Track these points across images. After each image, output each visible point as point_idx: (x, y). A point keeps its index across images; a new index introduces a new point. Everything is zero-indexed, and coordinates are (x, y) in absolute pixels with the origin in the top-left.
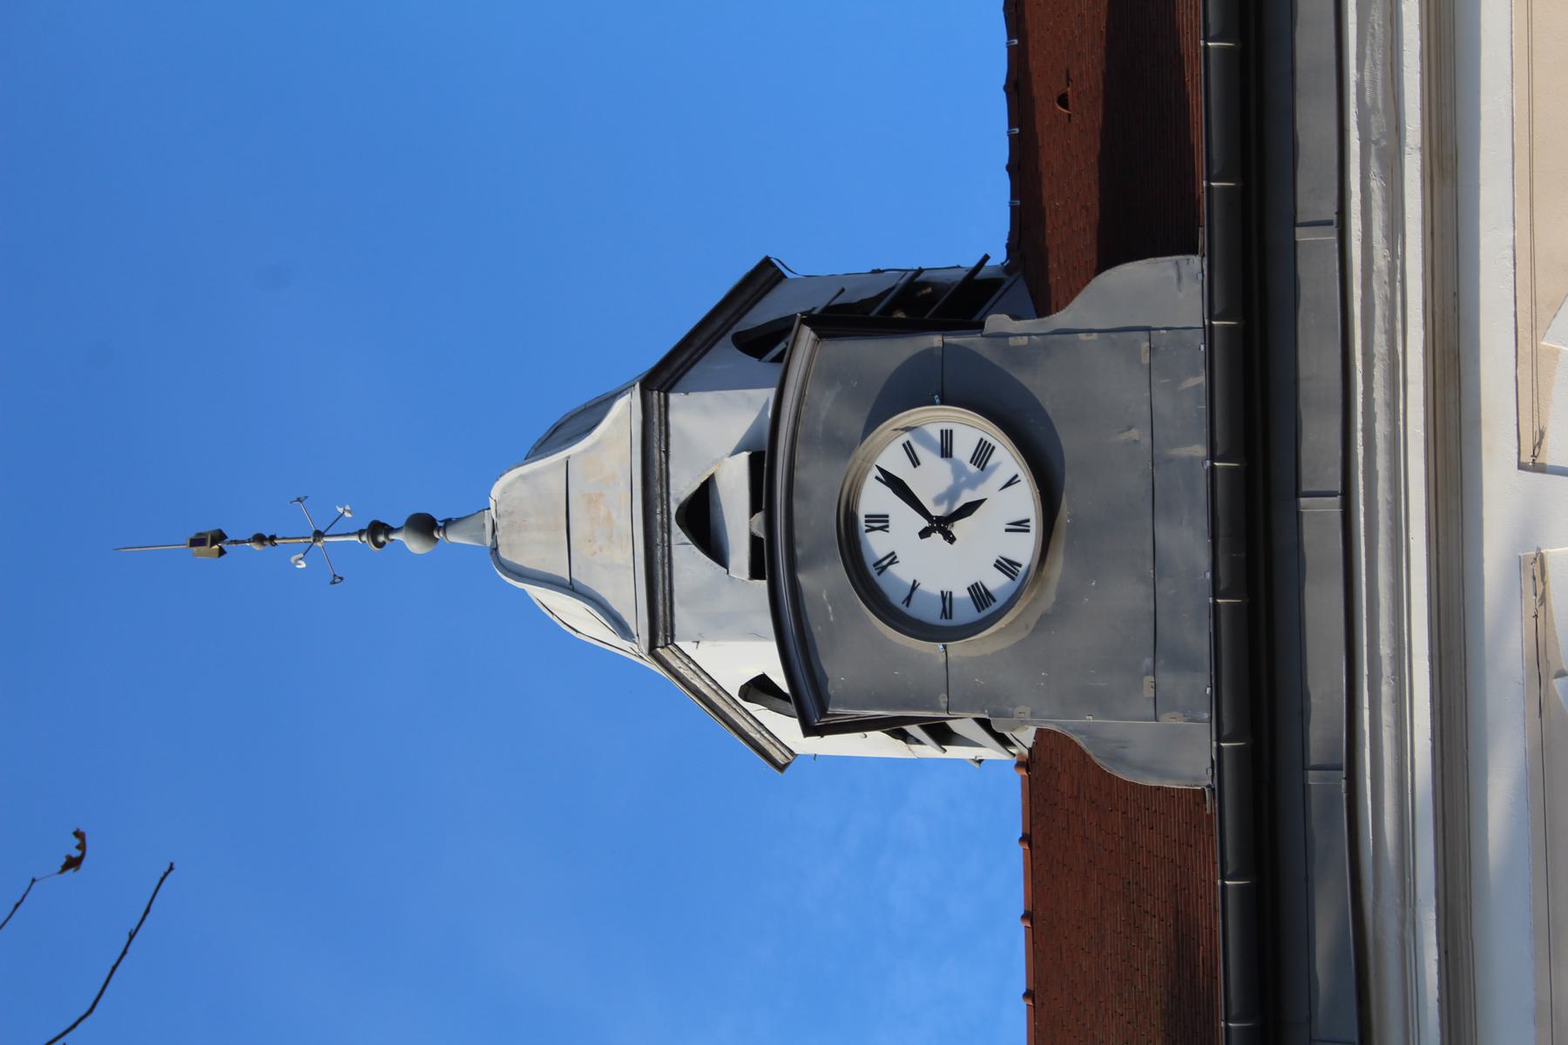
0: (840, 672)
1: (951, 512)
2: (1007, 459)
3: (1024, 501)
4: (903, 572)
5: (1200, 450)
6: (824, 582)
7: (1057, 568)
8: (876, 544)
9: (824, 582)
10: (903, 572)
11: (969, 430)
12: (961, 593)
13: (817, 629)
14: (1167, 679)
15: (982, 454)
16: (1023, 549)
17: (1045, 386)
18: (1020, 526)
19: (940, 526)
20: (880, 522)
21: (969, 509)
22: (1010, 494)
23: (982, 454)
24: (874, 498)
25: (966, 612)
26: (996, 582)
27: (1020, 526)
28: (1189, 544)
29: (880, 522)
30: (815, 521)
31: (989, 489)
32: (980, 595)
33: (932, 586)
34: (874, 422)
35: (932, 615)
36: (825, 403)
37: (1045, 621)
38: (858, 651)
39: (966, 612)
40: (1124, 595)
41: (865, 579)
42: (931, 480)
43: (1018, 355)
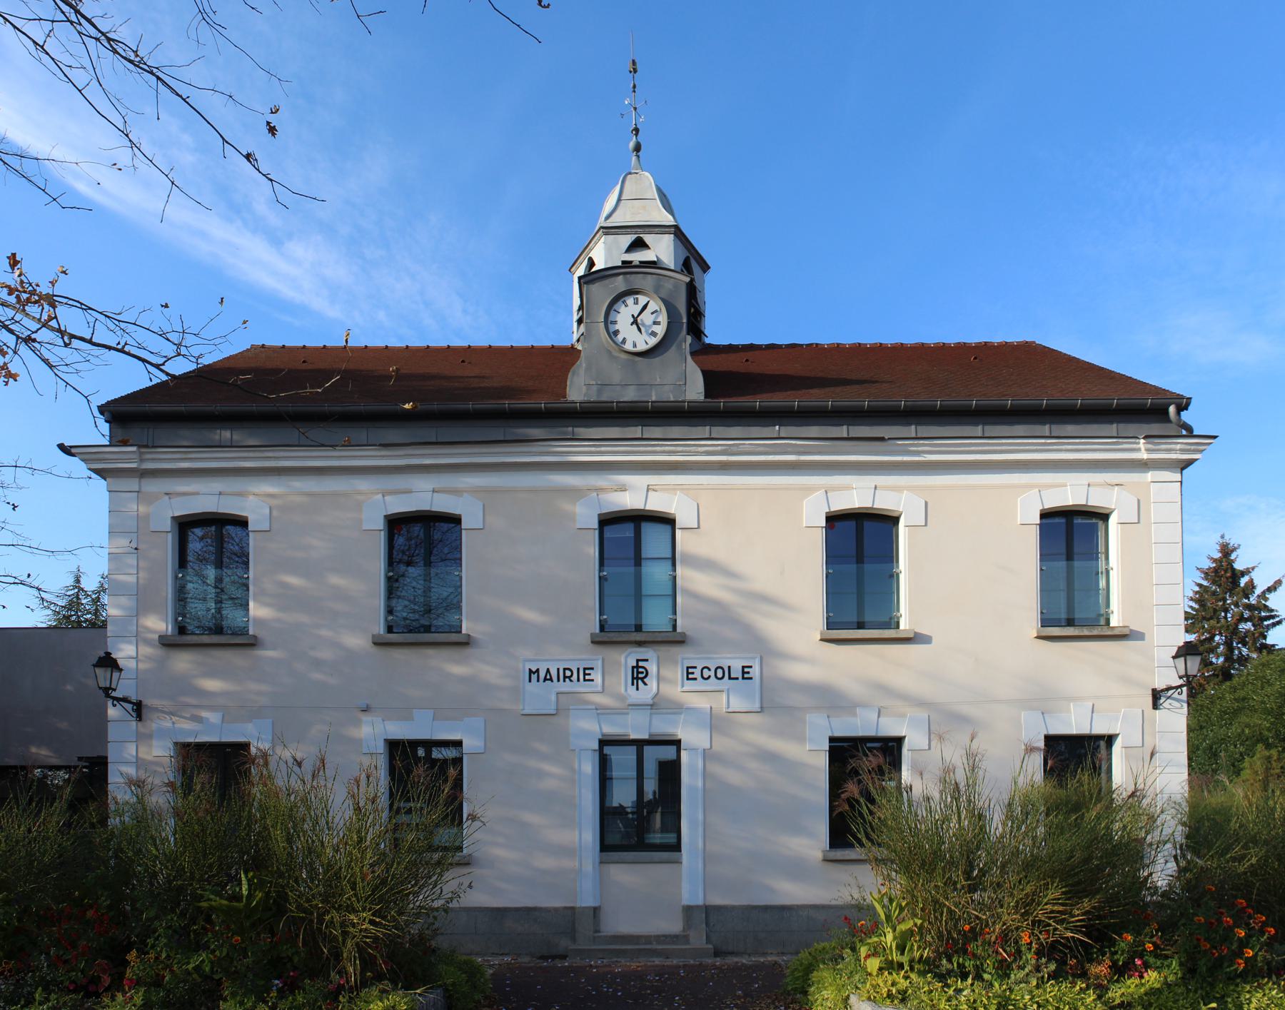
0: (595, 288)
1: (641, 321)
2: (653, 341)
3: (642, 347)
4: (622, 309)
5: (654, 399)
6: (620, 284)
7: (624, 356)
8: (630, 300)
9: (620, 284)
10: (622, 309)
11: (661, 330)
12: (617, 327)
13: (607, 281)
14: (595, 388)
15: (654, 334)
16: (628, 346)
17: (672, 353)
18: (635, 346)
19: (635, 322)
20: (636, 302)
21: (639, 330)
22: (643, 342)
23: (654, 334)
24: (643, 300)
25: (612, 328)
26: (620, 338)
27: (635, 346)
28: (630, 395)
29: (636, 302)
30: (638, 281)
31: (645, 336)
32: (616, 333)
33: (619, 318)
34: (663, 300)
35: (611, 318)
36: (668, 285)
37: (609, 352)
38: (601, 294)
39: (612, 328)
40: (616, 375)
41: (620, 297)
42: (647, 318)
43: (680, 347)
